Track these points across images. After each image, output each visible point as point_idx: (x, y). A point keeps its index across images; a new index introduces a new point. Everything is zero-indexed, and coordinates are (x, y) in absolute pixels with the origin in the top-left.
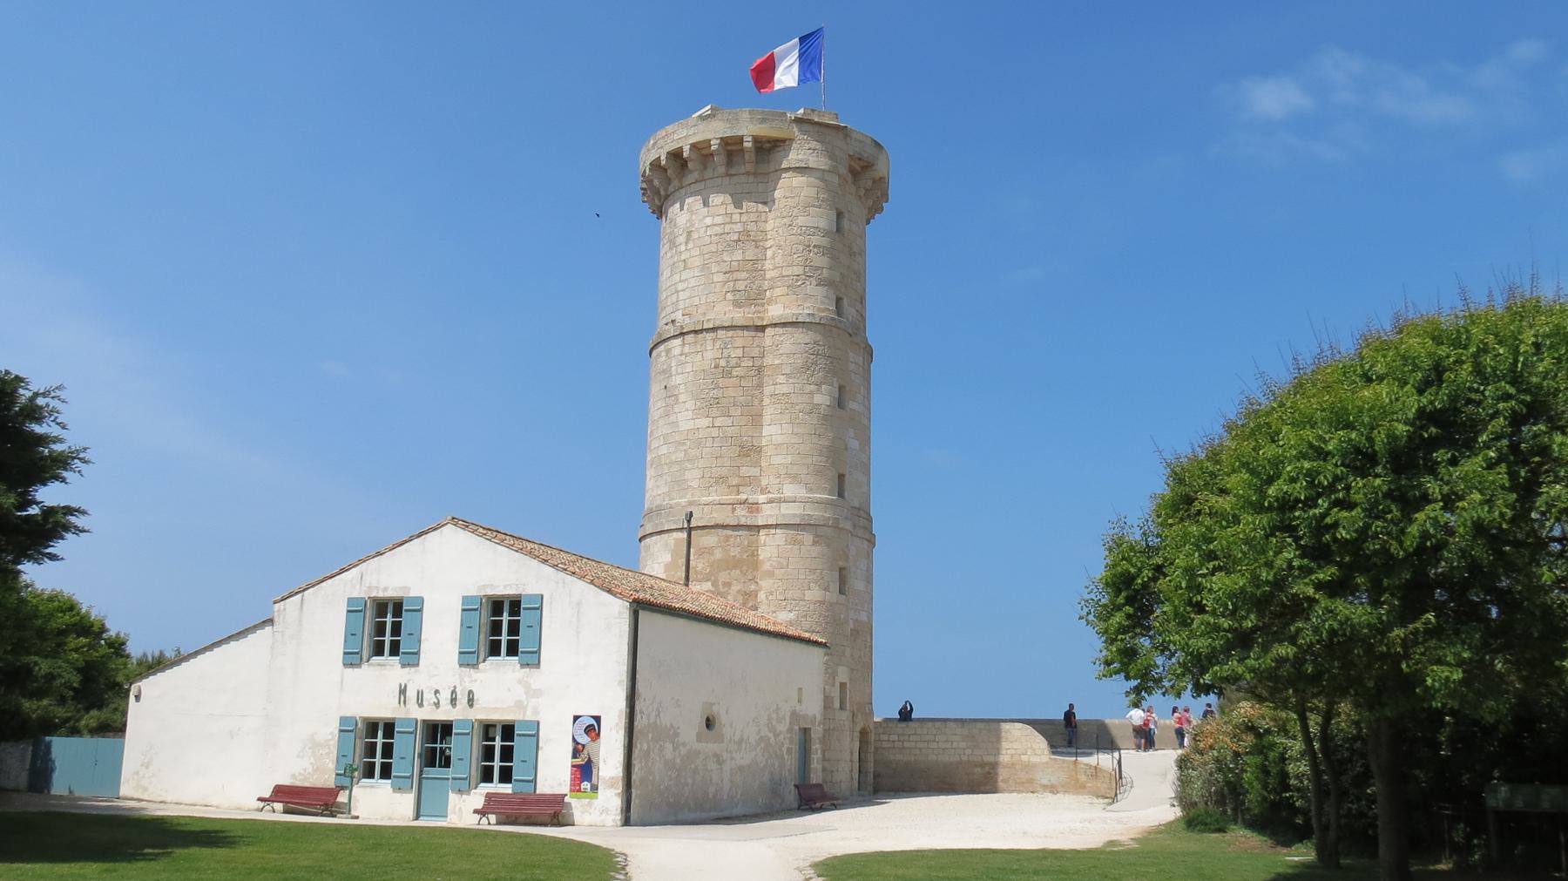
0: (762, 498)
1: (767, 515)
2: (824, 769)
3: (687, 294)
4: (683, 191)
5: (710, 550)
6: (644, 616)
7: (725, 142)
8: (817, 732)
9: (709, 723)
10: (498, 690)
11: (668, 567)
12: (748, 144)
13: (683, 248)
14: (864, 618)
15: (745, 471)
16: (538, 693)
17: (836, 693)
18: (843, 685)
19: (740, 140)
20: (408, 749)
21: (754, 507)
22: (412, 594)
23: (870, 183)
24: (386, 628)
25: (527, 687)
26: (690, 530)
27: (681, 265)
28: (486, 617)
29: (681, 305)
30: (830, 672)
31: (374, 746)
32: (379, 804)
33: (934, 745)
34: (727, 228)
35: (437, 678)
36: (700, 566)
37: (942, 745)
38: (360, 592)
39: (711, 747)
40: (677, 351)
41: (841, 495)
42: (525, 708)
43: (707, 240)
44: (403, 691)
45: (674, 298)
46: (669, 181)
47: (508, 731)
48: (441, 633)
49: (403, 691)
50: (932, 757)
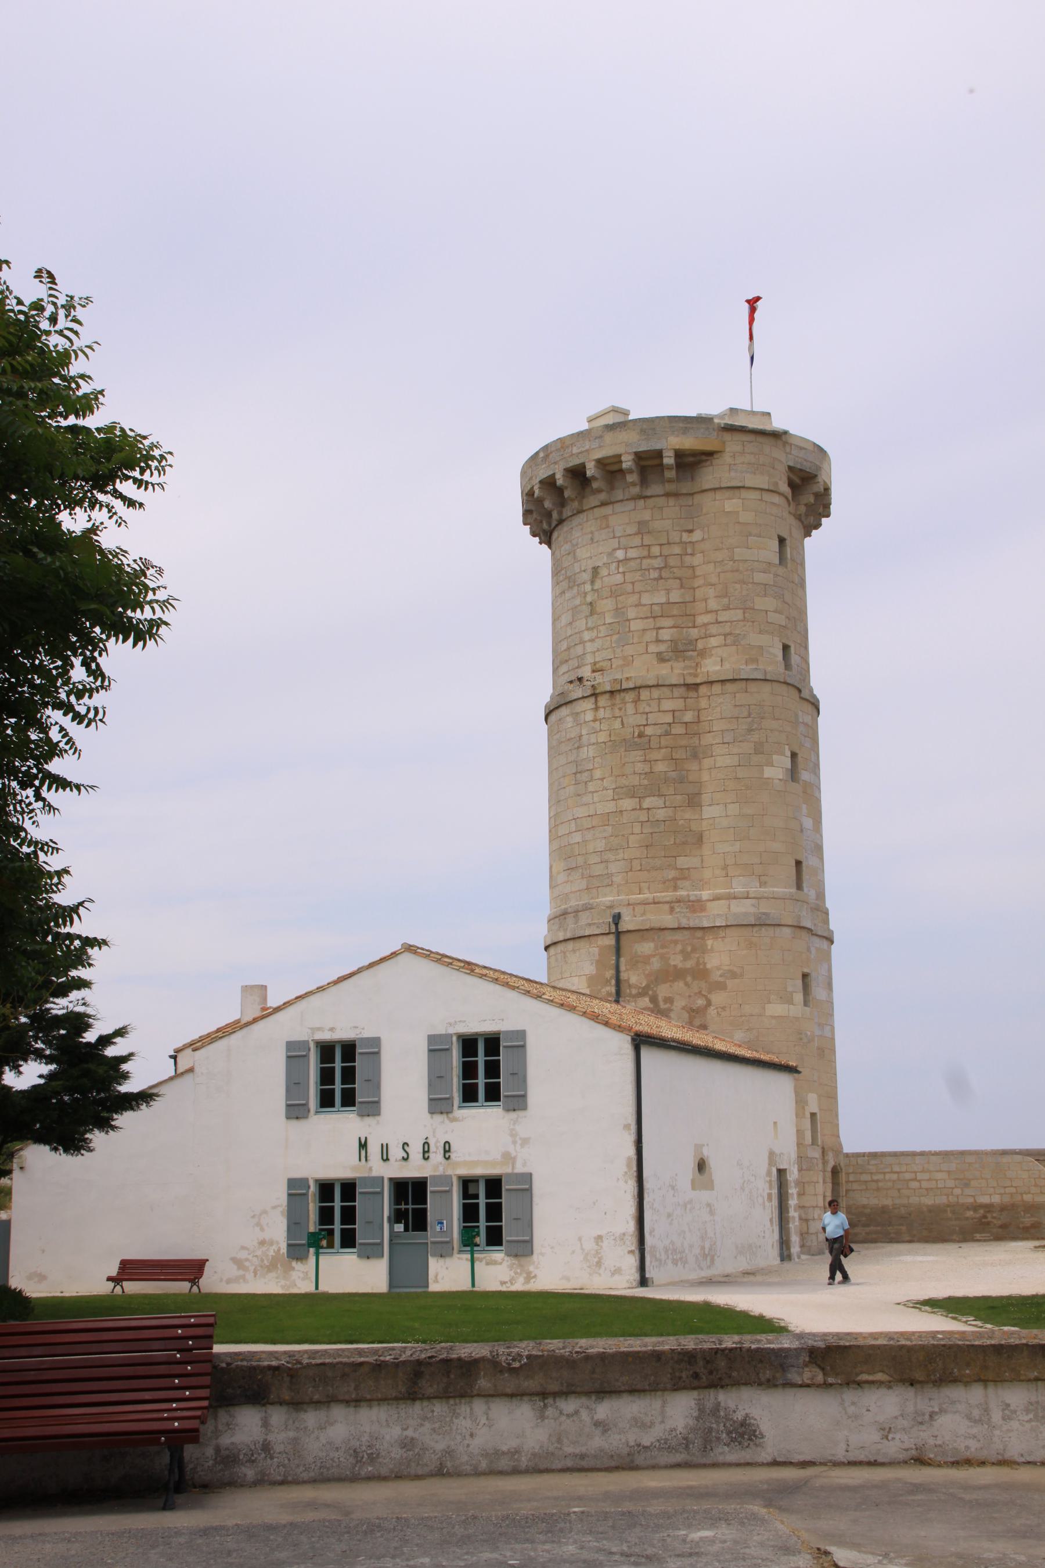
0: (705, 894)
1: (716, 913)
2: (801, 1219)
3: (598, 644)
4: (582, 517)
5: (646, 960)
6: (646, 1053)
7: (639, 456)
8: (793, 1175)
9: (701, 1166)
10: (480, 1141)
11: (592, 980)
12: (669, 460)
13: (588, 587)
14: (829, 1035)
15: (682, 862)
16: (525, 1141)
17: (807, 1123)
18: (813, 1115)
19: (659, 454)
20: (378, 1213)
21: (696, 906)
22: (367, 1034)
23: (812, 500)
25: (513, 1134)
26: (618, 934)
27: (586, 610)
29: (589, 659)
30: (800, 1102)
31: (332, 1212)
32: (354, 1274)
33: (914, 1185)
34: (646, 563)
35: (407, 1128)
36: (633, 980)
37: (925, 1185)
38: (301, 1034)
39: (704, 1196)
40: (589, 716)
41: (799, 886)
42: (513, 1160)
43: (619, 578)
44: (363, 1145)
45: (579, 650)
46: (562, 503)
47: (494, 1185)
48: (403, 1079)
49: (363, 1145)
50: (914, 1200)
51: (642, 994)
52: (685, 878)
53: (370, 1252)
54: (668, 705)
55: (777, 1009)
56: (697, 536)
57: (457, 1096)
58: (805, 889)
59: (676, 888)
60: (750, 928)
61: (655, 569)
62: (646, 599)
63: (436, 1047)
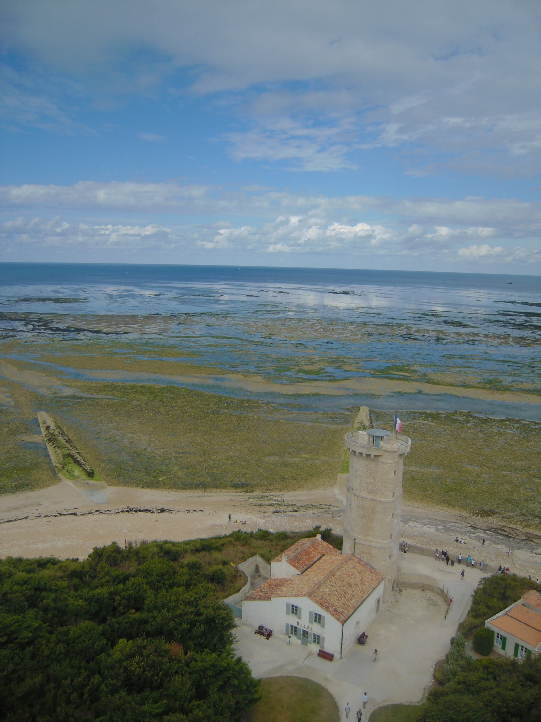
10: (316, 629)
24: (295, 610)
28: (314, 615)
44: (298, 623)
49: (298, 623)
53: (299, 638)
56: (377, 470)
57: (313, 621)
62: (366, 480)
63: (311, 613)
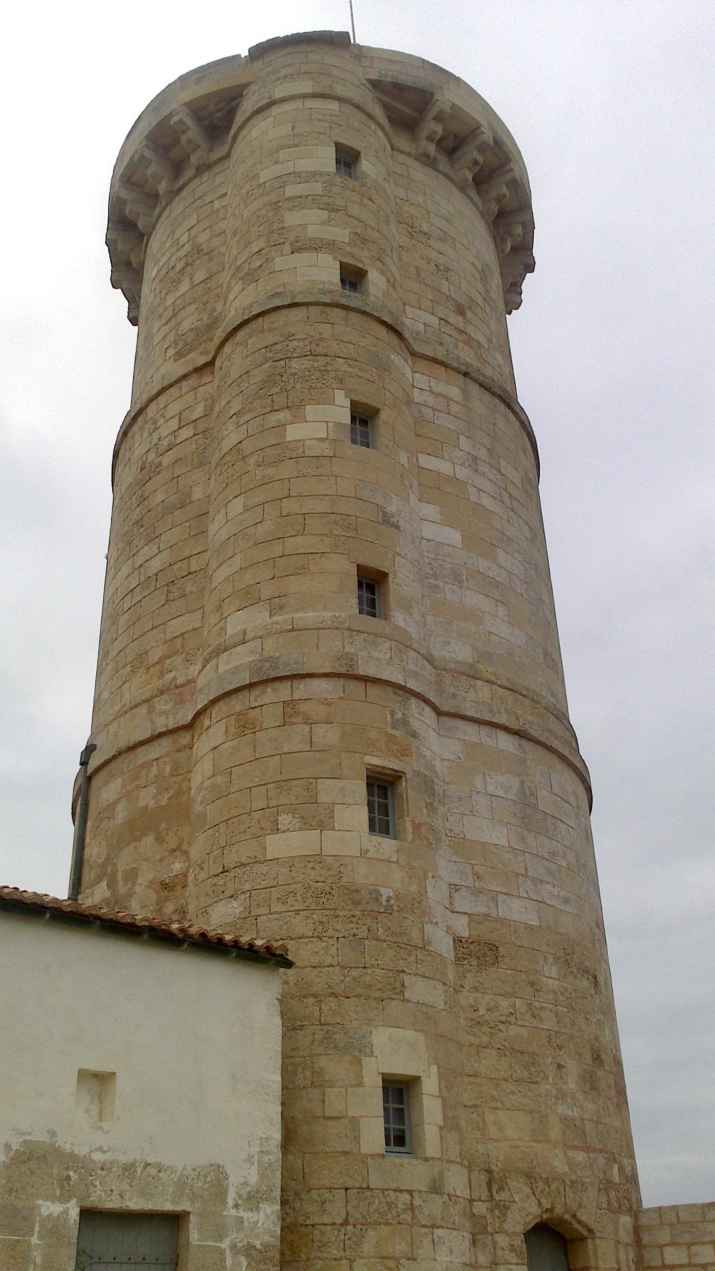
51: (99, 878)
52: (176, 653)
54: (175, 408)
55: (288, 842)
58: (399, 618)
59: (162, 674)
60: (246, 693)
61: (180, 259)
